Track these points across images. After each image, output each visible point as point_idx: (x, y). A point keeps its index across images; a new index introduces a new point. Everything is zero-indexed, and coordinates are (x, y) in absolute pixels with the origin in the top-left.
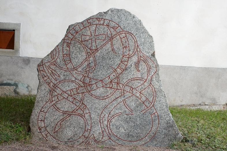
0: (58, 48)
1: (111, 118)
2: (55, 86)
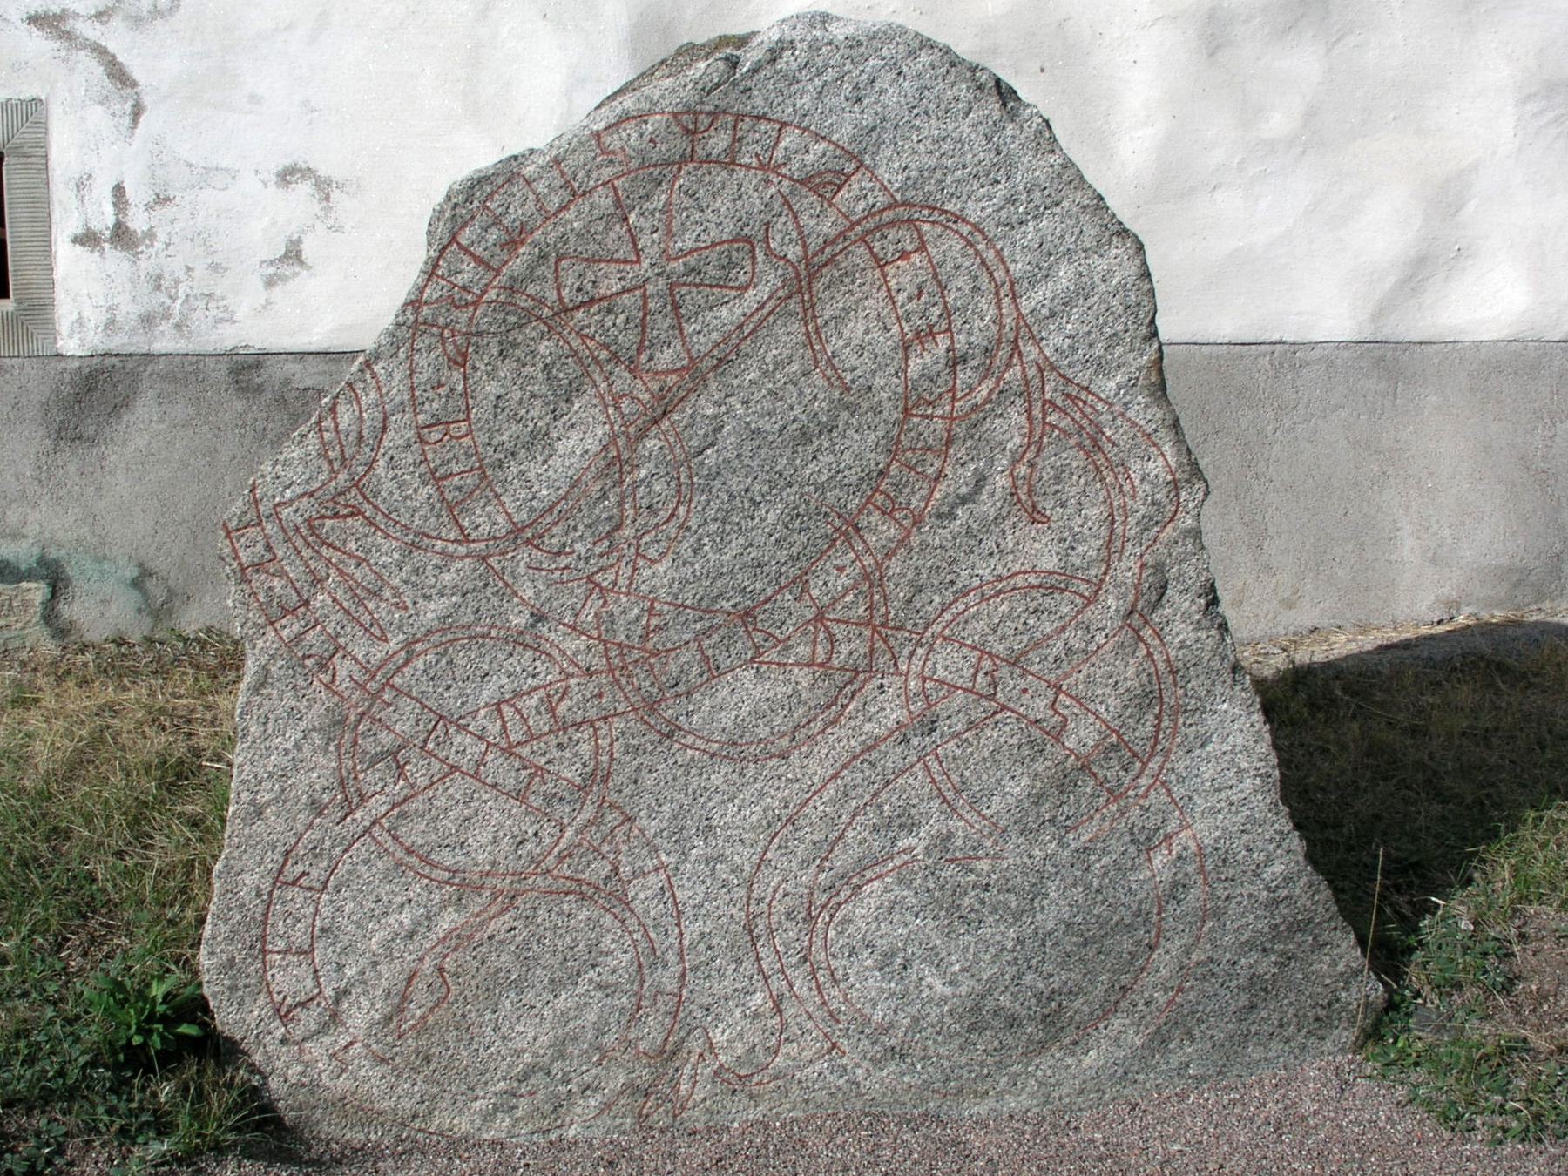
0: (374, 375)
1: (834, 900)
2: (379, 685)
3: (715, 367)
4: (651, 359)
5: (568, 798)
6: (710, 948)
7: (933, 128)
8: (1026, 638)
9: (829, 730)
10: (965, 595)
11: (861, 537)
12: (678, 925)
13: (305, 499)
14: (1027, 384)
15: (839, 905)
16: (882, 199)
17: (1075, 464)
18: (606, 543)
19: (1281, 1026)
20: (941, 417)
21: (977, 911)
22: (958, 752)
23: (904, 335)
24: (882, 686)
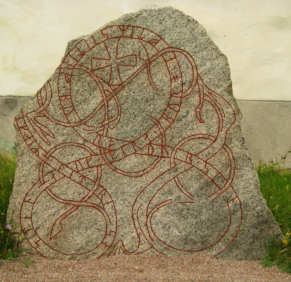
0: (50, 85)
1: (153, 211)
2: (48, 155)
3: (127, 84)
4: (112, 82)
5: (91, 184)
6: (123, 221)
7: (178, 30)
8: (198, 150)
9: (152, 170)
10: (185, 139)
11: (160, 125)
12: (116, 215)
13: (33, 112)
14: (200, 89)
15: (154, 212)
16: (166, 46)
17: (210, 109)
18: (101, 124)
19: (261, 247)
20: (179, 97)
21: (186, 215)
22: (182, 176)
23: (171, 78)
24: (164, 160)
